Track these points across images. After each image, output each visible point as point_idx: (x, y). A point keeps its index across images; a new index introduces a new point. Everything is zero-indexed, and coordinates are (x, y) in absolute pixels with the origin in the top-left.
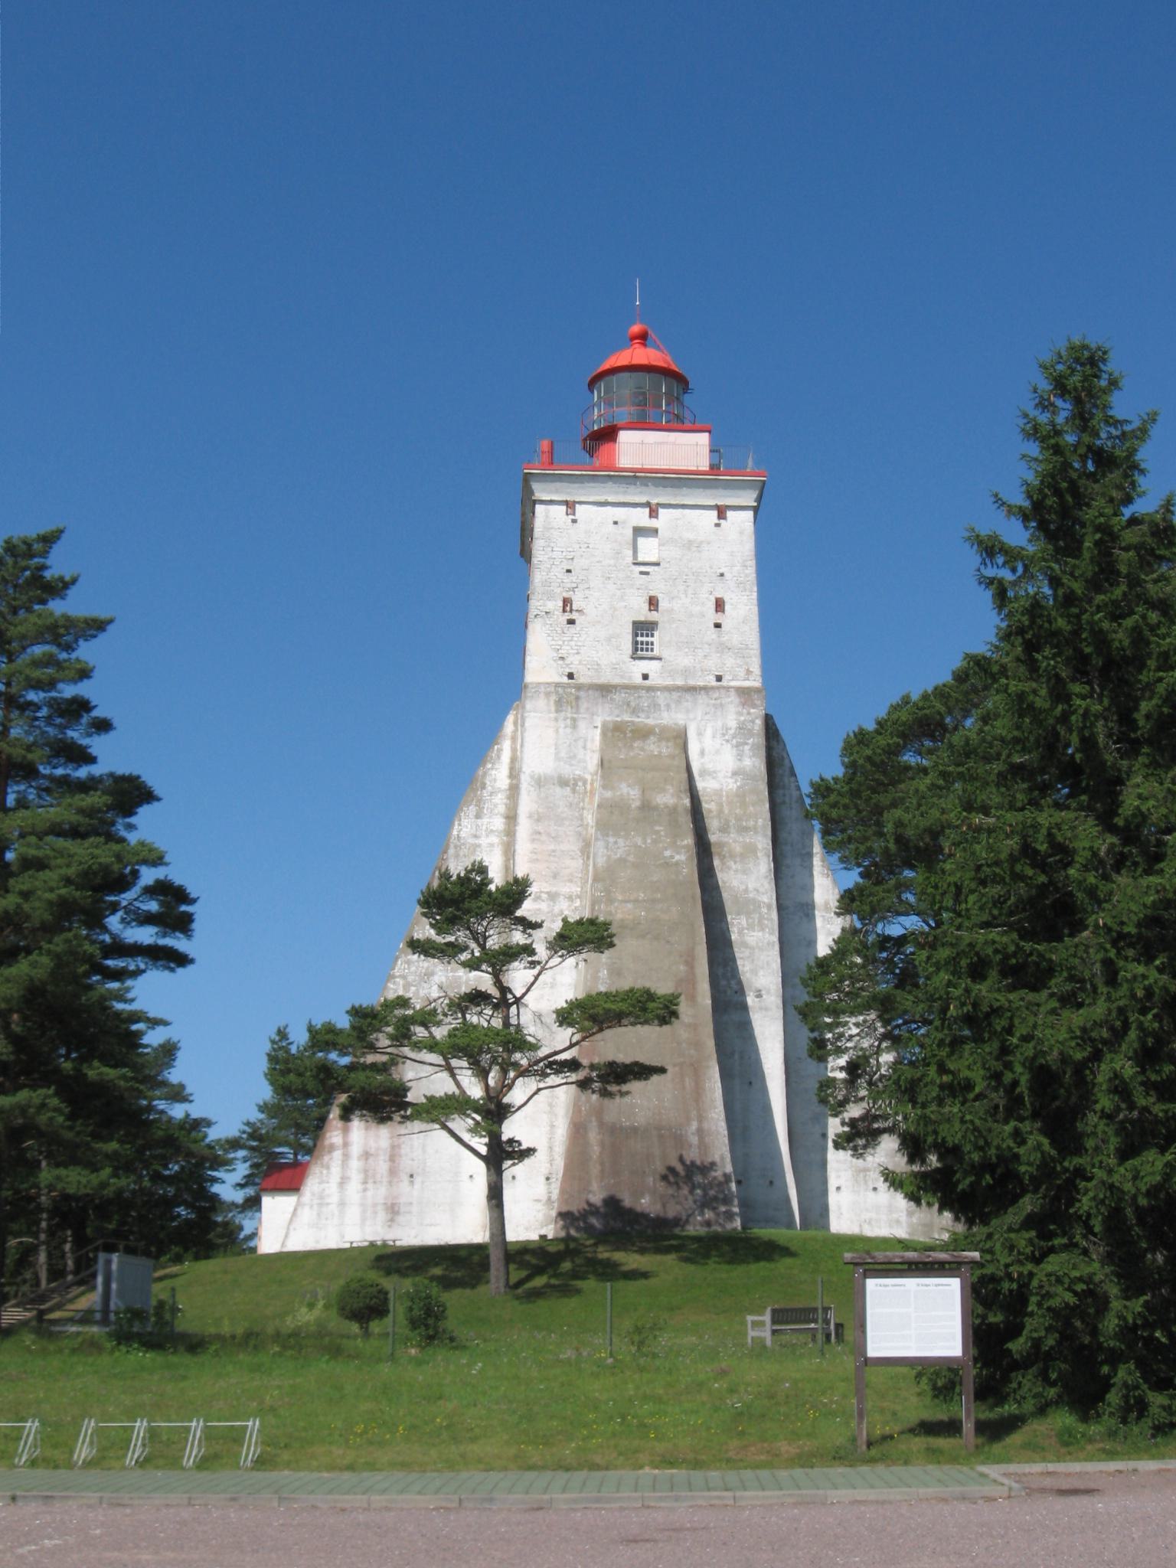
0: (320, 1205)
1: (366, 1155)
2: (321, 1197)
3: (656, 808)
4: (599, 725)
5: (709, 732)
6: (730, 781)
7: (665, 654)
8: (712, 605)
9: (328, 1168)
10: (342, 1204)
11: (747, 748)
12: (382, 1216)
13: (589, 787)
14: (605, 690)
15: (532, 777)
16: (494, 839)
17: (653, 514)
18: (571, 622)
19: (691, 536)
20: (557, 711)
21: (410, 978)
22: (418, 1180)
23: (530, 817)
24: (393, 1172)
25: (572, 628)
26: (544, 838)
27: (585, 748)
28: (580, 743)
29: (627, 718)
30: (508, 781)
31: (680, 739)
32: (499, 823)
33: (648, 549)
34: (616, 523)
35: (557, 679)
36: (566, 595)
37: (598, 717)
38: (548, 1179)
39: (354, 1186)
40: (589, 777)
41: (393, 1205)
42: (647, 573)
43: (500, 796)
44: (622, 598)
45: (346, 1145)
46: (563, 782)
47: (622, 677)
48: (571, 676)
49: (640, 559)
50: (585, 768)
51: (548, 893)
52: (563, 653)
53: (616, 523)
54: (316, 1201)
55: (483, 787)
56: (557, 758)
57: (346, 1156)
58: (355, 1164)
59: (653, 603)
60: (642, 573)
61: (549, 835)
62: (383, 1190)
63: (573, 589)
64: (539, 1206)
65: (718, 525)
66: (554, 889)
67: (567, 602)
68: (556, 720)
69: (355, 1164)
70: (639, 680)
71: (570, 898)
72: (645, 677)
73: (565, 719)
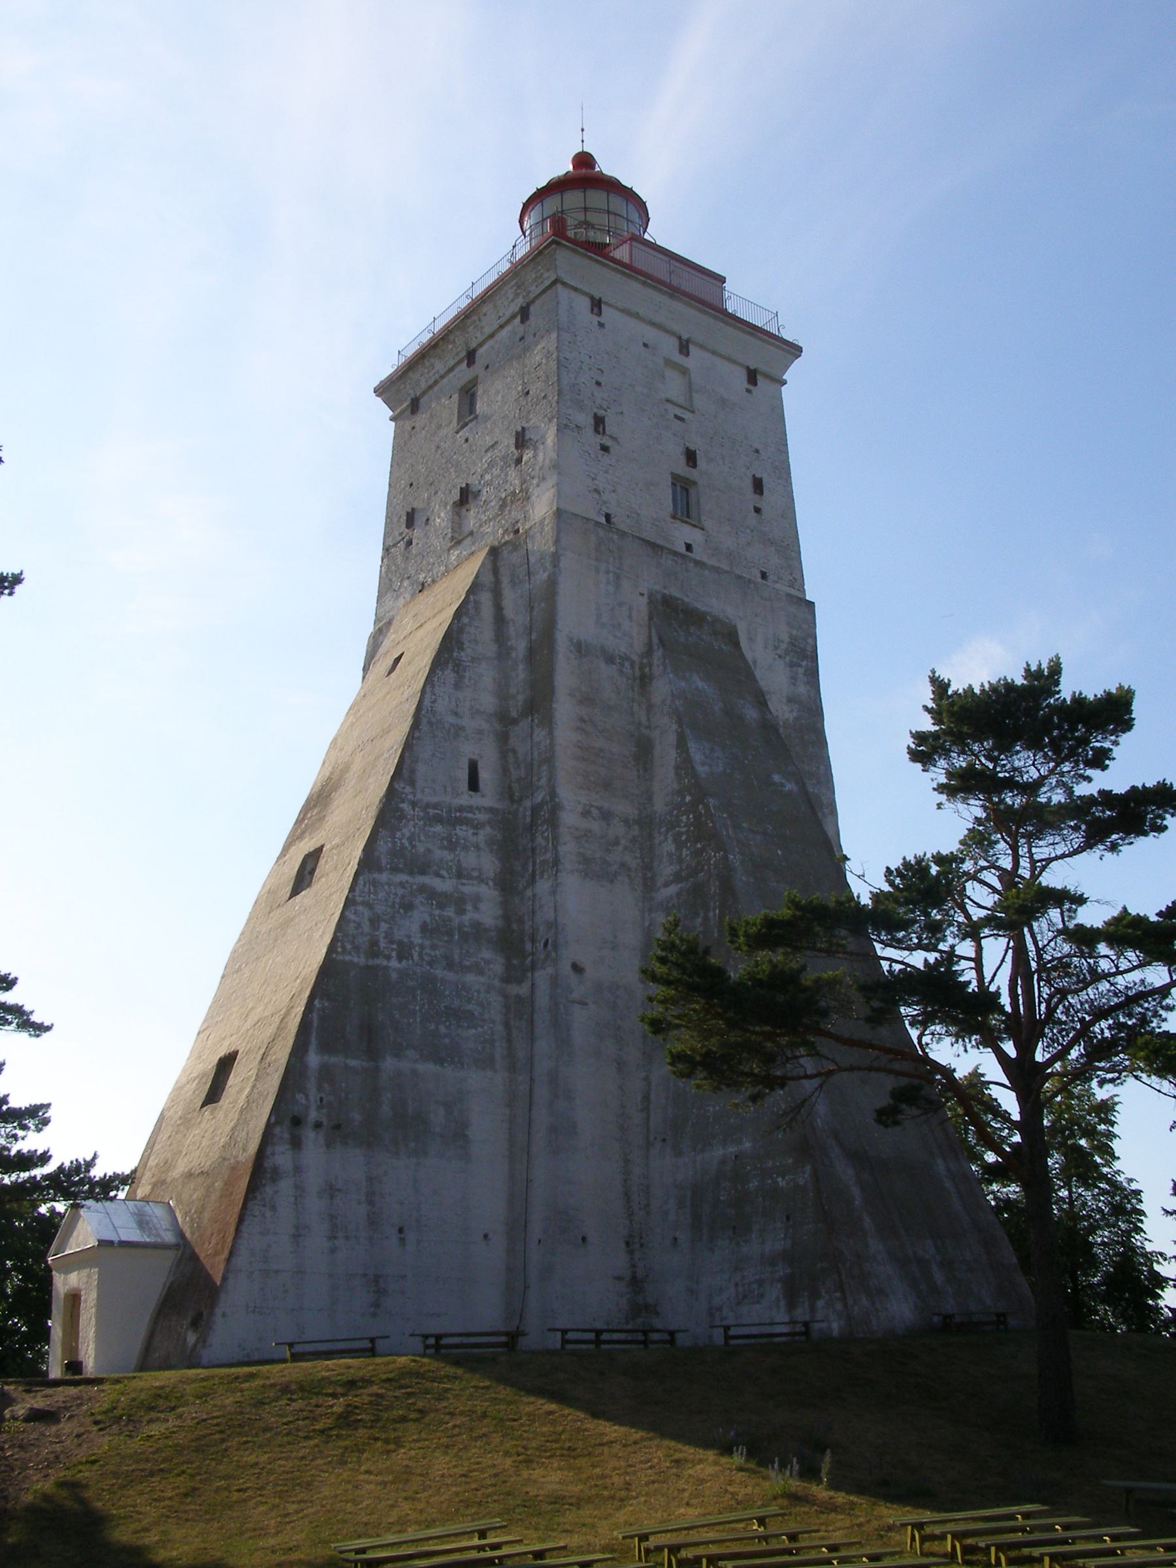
1: (331, 1190)
4: (646, 593)
6: (785, 708)
8: (748, 484)
9: (274, 1208)
13: (638, 673)
15: (571, 640)
16: (485, 726)
17: (684, 348)
21: (380, 909)
23: (571, 695)
25: (606, 459)
27: (630, 617)
29: (674, 592)
31: (732, 637)
34: (645, 345)
35: (593, 515)
36: (601, 413)
37: (650, 578)
38: (627, 1244)
40: (635, 658)
41: (377, 1278)
45: (298, 1169)
46: (610, 660)
48: (608, 517)
51: (599, 808)
53: (645, 345)
55: (461, 648)
57: (300, 1190)
59: (691, 457)
60: (676, 416)
68: (597, 570)
70: (683, 550)
71: (626, 822)
73: (608, 572)
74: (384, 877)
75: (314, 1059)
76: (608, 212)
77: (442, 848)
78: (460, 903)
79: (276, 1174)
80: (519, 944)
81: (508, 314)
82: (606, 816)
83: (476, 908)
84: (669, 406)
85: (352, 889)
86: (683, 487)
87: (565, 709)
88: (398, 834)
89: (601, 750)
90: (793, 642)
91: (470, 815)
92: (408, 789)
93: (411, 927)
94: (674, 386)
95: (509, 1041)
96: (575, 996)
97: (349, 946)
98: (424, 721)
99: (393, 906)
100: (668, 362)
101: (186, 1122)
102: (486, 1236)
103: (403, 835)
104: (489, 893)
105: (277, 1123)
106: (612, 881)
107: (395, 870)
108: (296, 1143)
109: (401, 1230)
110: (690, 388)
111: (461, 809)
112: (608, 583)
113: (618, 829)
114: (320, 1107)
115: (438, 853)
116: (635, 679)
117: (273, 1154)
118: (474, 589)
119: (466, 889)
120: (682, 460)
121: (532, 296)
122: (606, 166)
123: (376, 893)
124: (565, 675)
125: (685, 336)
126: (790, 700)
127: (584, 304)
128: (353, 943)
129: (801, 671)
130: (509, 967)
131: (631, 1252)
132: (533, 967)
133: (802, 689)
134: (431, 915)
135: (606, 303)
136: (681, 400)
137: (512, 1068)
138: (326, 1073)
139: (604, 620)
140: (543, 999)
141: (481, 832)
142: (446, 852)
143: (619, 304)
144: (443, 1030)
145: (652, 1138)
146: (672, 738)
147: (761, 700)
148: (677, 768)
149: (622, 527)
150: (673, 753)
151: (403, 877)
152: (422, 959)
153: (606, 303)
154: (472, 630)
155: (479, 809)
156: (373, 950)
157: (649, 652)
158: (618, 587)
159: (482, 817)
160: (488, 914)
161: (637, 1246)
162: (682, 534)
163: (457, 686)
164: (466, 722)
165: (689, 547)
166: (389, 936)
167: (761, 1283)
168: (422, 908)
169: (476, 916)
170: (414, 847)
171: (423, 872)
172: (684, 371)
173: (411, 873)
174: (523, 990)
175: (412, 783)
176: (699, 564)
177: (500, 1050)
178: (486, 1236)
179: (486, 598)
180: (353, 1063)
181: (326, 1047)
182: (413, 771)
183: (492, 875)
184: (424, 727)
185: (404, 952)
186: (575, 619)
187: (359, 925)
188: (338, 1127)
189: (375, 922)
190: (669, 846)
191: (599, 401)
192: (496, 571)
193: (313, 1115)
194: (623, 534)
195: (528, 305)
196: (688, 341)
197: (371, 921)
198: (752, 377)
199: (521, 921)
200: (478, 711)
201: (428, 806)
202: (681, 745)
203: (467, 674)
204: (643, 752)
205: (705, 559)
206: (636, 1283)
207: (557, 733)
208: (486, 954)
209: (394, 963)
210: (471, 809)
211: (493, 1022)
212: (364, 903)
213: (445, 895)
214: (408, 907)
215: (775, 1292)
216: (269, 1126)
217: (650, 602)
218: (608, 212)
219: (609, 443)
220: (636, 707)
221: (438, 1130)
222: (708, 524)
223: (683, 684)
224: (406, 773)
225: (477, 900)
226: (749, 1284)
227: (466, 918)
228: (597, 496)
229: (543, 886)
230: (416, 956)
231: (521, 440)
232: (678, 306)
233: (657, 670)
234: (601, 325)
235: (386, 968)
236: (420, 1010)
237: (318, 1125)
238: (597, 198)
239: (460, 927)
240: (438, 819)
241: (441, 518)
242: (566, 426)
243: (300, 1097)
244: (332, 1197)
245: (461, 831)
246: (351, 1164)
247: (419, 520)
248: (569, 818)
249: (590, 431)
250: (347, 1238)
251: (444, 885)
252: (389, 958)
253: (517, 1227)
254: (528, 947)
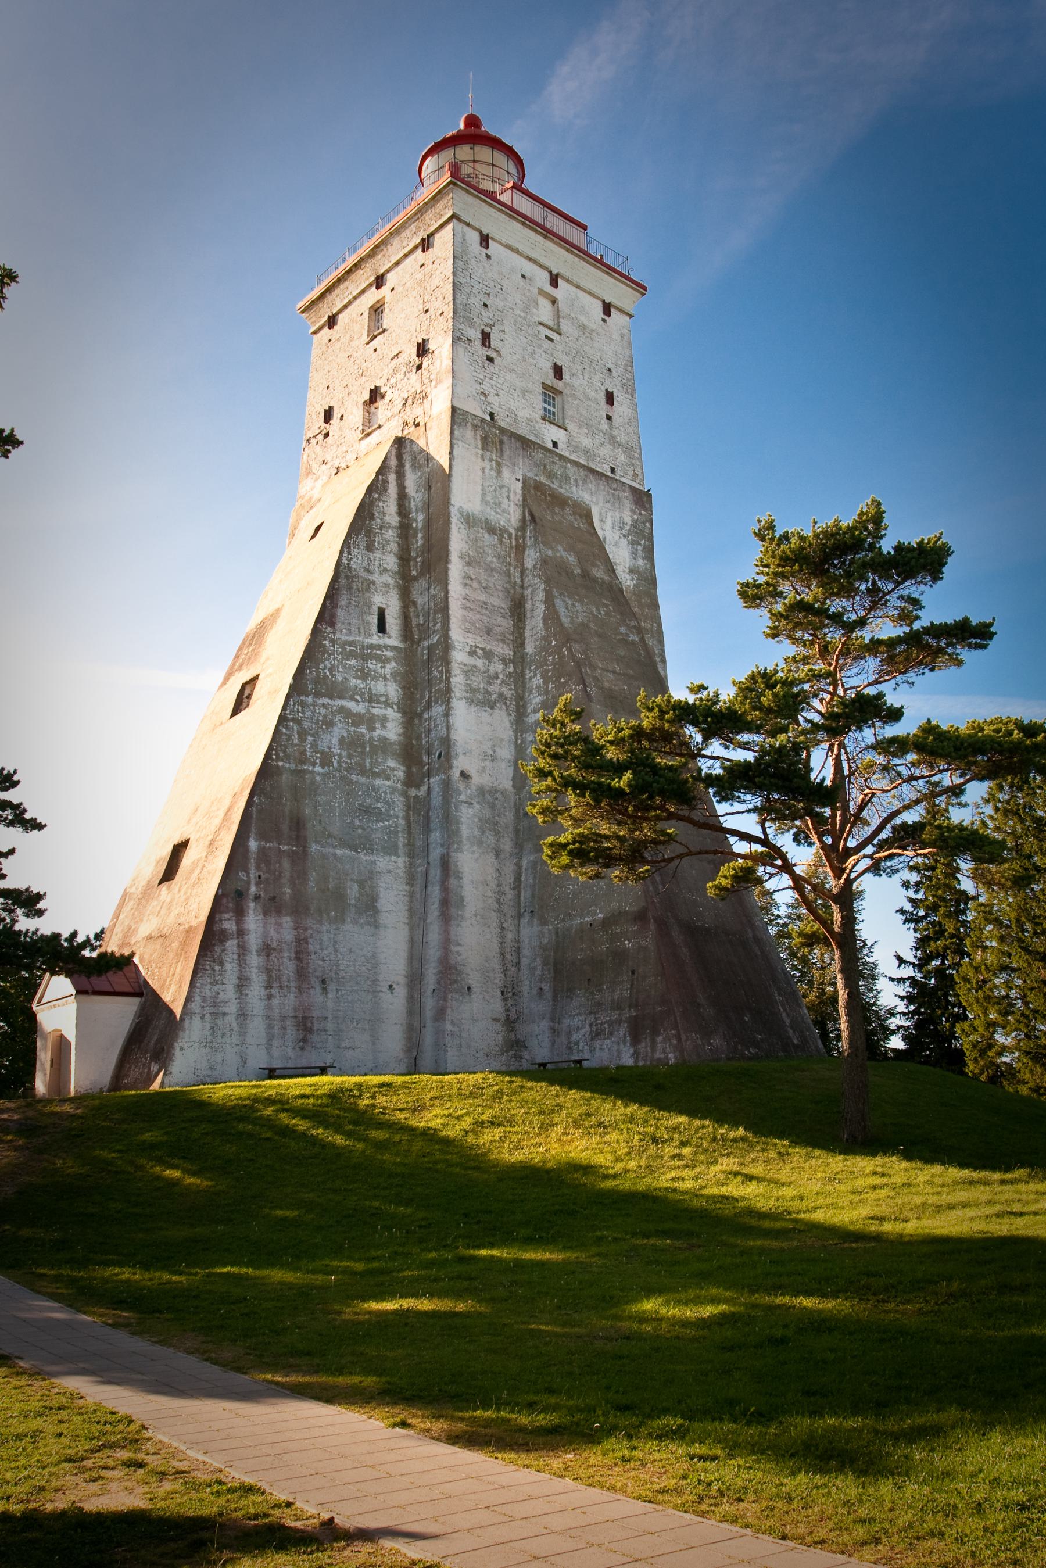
0: (215, 1015)
1: (267, 950)
2: (215, 1005)
3: (595, 580)
5: (609, 521)
6: (628, 576)
7: (569, 427)
8: (602, 396)
9: (221, 964)
10: (242, 1015)
11: (640, 548)
12: (292, 1033)
13: (514, 543)
14: (526, 444)
15: (461, 513)
16: (391, 581)
19: (583, 319)
20: (483, 449)
22: (332, 987)
24: (302, 974)
25: (491, 368)
26: (475, 585)
27: (508, 498)
28: (505, 490)
29: (543, 479)
30: (397, 519)
31: (588, 516)
32: (391, 562)
34: (523, 276)
35: (479, 413)
36: (487, 329)
38: (502, 993)
39: (256, 991)
40: (513, 532)
41: (305, 1018)
42: (552, 340)
43: (390, 532)
44: (532, 354)
45: (241, 933)
46: (491, 530)
47: (536, 436)
48: (492, 415)
50: (509, 521)
51: (483, 649)
52: (486, 387)
53: (523, 276)
54: (208, 1010)
56: (483, 500)
57: (243, 950)
58: (254, 960)
59: (558, 371)
61: (480, 582)
62: (291, 999)
63: (491, 326)
64: (499, 1027)
66: (488, 647)
67: (486, 338)
68: (483, 458)
69: (254, 960)
70: (550, 445)
71: (504, 661)
73: (491, 460)
74: (310, 699)
75: (253, 844)
76: (493, 165)
77: (357, 677)
78: (370, 721)
79: (224, 936)
80: (424, 754)
81: (412, 245)
82: (488, 655)
83: (384, 727)
84: (541, 328)
85: (284, 708)
86: (550, 393)
87: (456, 569)
88: (321, 666)
89: (485, 603)
90: (635, 524)
91: (379, 652)
92: (329, 629)
93: (332, 740)
94: (544, 312)
95: (409, 833)
96: (463, 797)
97: (281, 754)
98: (343, 575)
99: (317, 723)
100: (541, 292)
101: (147, 894)
102: (391, 986)
103: (325, 667)
104: (393, 714)
105: (223, 895)
106: (492, 708)
107: (317, 695)
108: (240, 913)
109: (323, 981)
110: (558, 315)
111: (371, 647)
112: (491, 469)
113: (497, 667)
114: (257, 884)
115: (354, 682)
116: (511, 547)
117: (221, 920)
118: (383, 470)
119: (375, 711)
120: (551, 372)
121: (432, 229)
122: (488, 127)
123: (303, 712)
124: (458, 542)
125: (555, 272)
126: (631, 571)
127: (475, 237)
128: (284, 752)
129: (640, 548)
130: (409, 774)
131: (505, 1000)
132: (429, 775)
133: (641, 562)
134: (348, 731)
135: (492, 239)
136: (551, 323)
137: (411, 855)
138: (263, 855)
139: (488, 498)
140: (436, 800)
141: (387, 666)
142: (359, 681)
143: (503, 241)
144: (357, 822)
145: (522, 910)
146: (541, 595)
147: (611, 569)
148: (545, 620)
149: (503, 424)
150: (541, 608)
151: (326, 701)
152: (341, 766)
153: (492, 239)
154: (381, 504)
155: (386, 647)
156: (302, 759)
157: (522, 528)
158: (499, 472)
159: (389, 654)
160: (392, 731)
161: (510, 995)
162: (551, 434)
163: (370, 548)
164: (376, 577)
165: (555, 444)
166: (314, 746)
167: (611, 1023)
168: (340, 725)
169: (383, 733)
170: (334, 676)
171: (341, 697)
172: (554, 302)
173: (331, 698)
174: (422, 792)
175: (332, 624)
176: (562, 457)
177: (401, 840)
178: (391, 986)
179: (392, 478)
180: (285, 848)
181: (262, 836)
182: (333, 616)
183: (396, 700)
184: (343, 581)
185: (326, 759)
186: (466, 496)
187: (289, 738)
188: (273, 899)
189: (303, 734)
190: (538, 681)
191: (486, 320)
192: (400, 457)
193: (253, 889)
194: (503, 431)
195: (431, 235)
196: (557, 275)
197: (298, 732)
198: (607, 309)
199: (419, 738)
200: (385, 570)
201: (346, 643)
202: (549, 601)
203: (377, 539)
204: (518, 610)
205: (567, 454)
206: (510, 1023)
207: (450, 587)
208: (391, 763)
209: (318, 769)
210: (379, 647)
211: (397, 817)
212: (293, 720)
213: (358, 715)
214: (330, 724)
215: (622, 1030)
216: (217, 900)
217: (524, 488)
218: (493, 165)
219: (493, 355)
220: (512, 570)
221: (353, 902)
222: (570, 426)
223: (550, 553)
224: (327, 616)
225: (384, 720)
226: (602, 1024)
227: (375, 734)
228: (483, 398)
229: (438, 710)
230: (335, 764)
231: (422, 350)
232: (549, 245)
233: (529, 542)
234: (488, 257)
235: (312, 772)
236: (339, 806)
237: (257, 898)
238: (484, 153)
239: (371, 739)
240: (352, 655)
241: (355, 415)
242: (459, 339)
243: (242, 875)
244: (268, 956)
245: (371, 665)
246: (285, 930)
247: (336, 415)
248: (459, 657)
249: (478, 343)
250: (281, 987)
251: (358, 707)
252: (314, 764)
253: (415, 979)
254: (425, 758)
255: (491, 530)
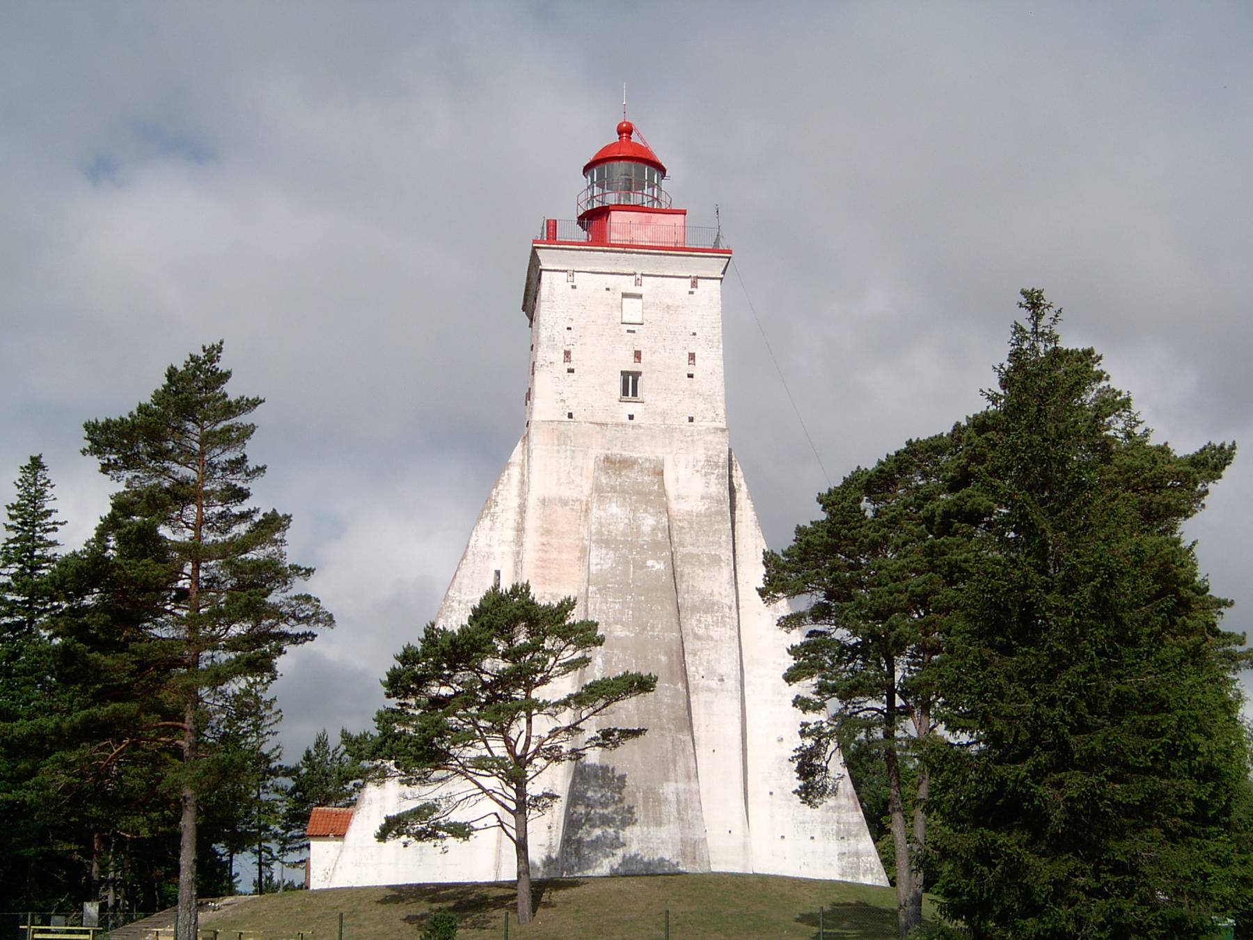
13: (584, 507)
17: (638, 283)
18: (571, 371)
19: (669, 302)
32: (510, 535)
33: (632, 310)
36: (567, 349)
40: (584, 499)
49: (625, 320)
52: (564, 396)
59: (638, 355)
65: (691, 293)
67: (567, 354)
72: (631, 417)
255: (564, 503)
